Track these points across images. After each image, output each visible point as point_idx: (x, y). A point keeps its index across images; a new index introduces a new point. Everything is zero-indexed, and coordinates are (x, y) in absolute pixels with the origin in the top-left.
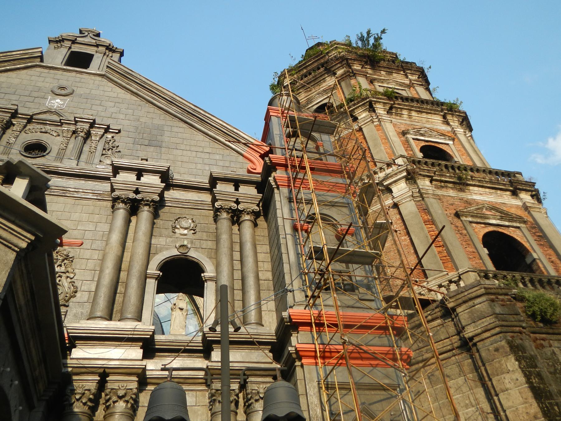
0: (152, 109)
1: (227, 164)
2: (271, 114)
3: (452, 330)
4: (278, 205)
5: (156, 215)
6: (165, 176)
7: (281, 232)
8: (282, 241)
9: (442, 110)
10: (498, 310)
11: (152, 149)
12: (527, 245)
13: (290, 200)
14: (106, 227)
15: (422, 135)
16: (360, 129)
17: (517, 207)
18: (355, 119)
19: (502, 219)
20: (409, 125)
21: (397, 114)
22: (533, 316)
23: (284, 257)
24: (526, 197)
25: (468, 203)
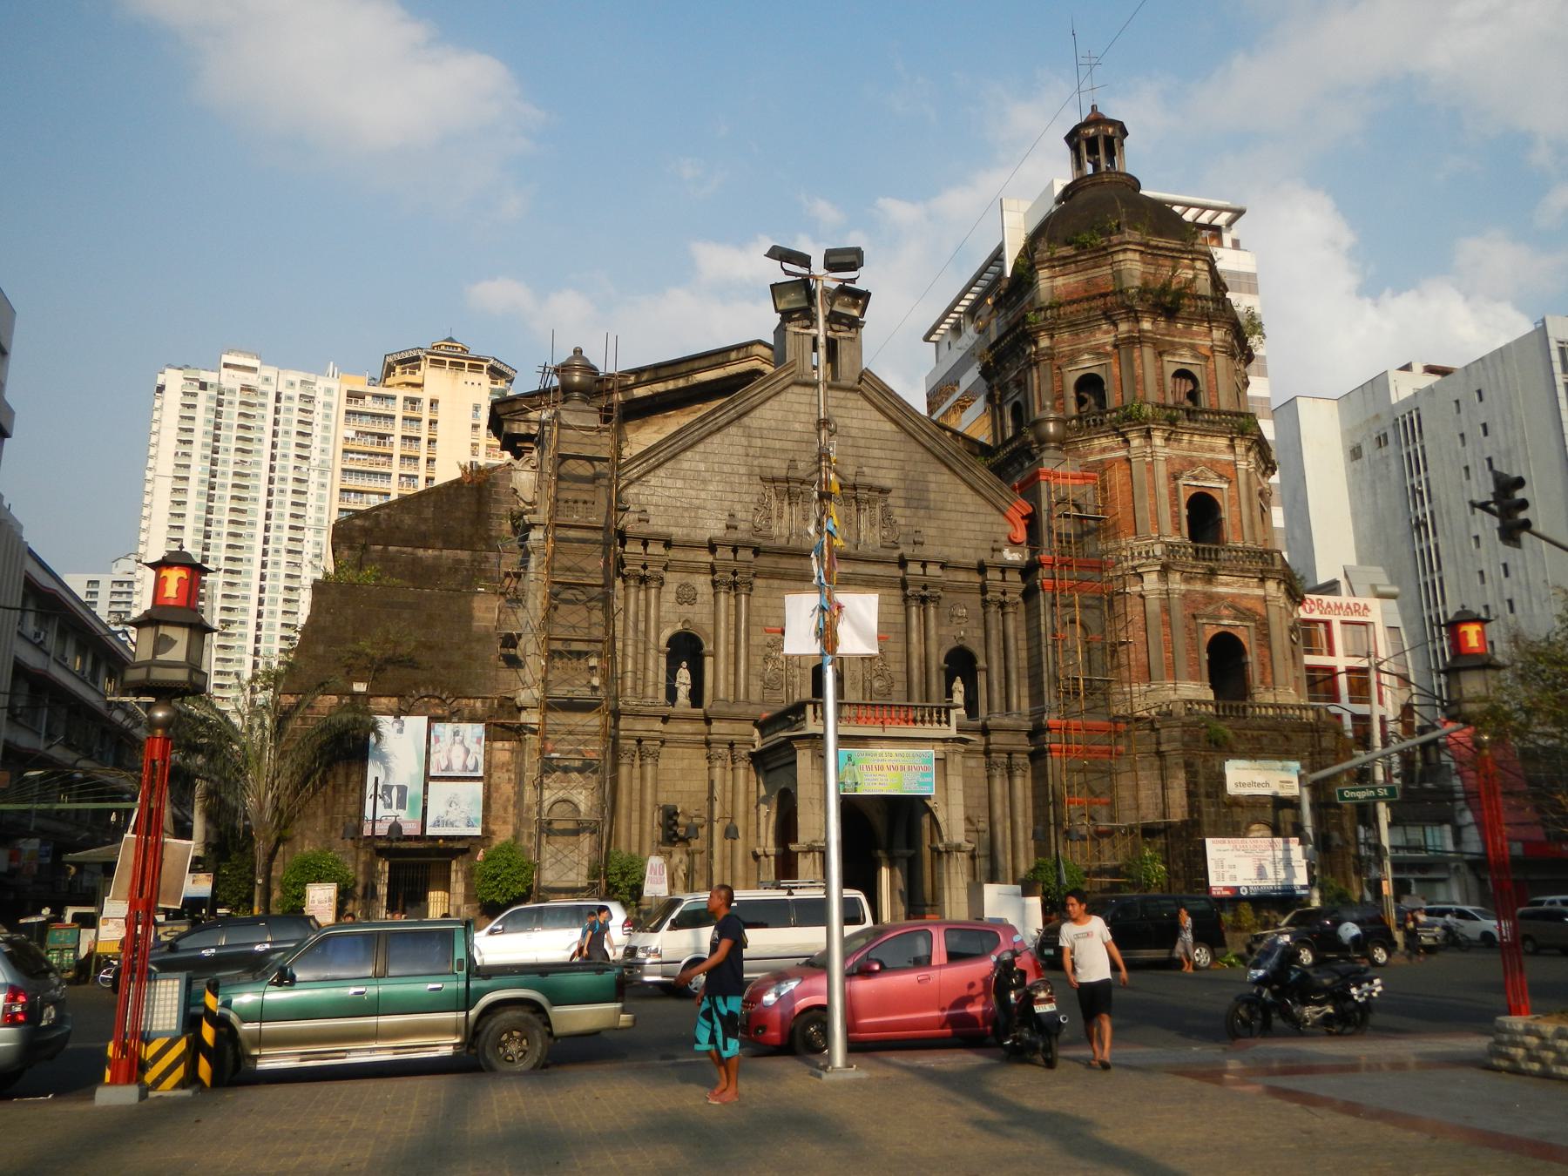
0: (913, 446)
1: (988, 528)
2: (1042, 477)
3: (1154, 740)
4: (1042, 602)
5: (936, 608)
6: (943, 566)
7: (1044, 641)
8: (1044, 650)
9: (1231, 433)
10: (1186, 738)
11: (922, 512)
12: (1247, 646)
13: (1054, 605)
14: (901, 619)
15: (1196, 478)
16: (1128, 460)
17: (1258, 597)
18: (1127, 441)
19: (1235, 618)
20: (1185, 458)
21: (1175, 440)
22: (1210, 741)
23: (1045, 665)
24: (1271, 586)
25: (1211, 598)
